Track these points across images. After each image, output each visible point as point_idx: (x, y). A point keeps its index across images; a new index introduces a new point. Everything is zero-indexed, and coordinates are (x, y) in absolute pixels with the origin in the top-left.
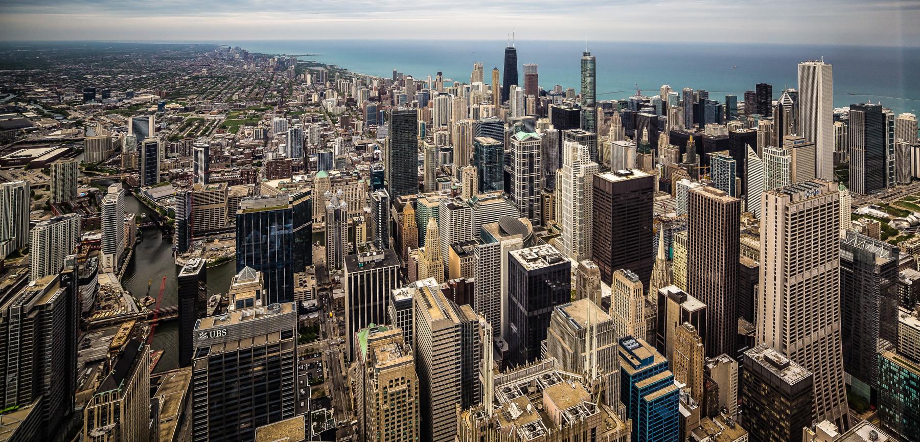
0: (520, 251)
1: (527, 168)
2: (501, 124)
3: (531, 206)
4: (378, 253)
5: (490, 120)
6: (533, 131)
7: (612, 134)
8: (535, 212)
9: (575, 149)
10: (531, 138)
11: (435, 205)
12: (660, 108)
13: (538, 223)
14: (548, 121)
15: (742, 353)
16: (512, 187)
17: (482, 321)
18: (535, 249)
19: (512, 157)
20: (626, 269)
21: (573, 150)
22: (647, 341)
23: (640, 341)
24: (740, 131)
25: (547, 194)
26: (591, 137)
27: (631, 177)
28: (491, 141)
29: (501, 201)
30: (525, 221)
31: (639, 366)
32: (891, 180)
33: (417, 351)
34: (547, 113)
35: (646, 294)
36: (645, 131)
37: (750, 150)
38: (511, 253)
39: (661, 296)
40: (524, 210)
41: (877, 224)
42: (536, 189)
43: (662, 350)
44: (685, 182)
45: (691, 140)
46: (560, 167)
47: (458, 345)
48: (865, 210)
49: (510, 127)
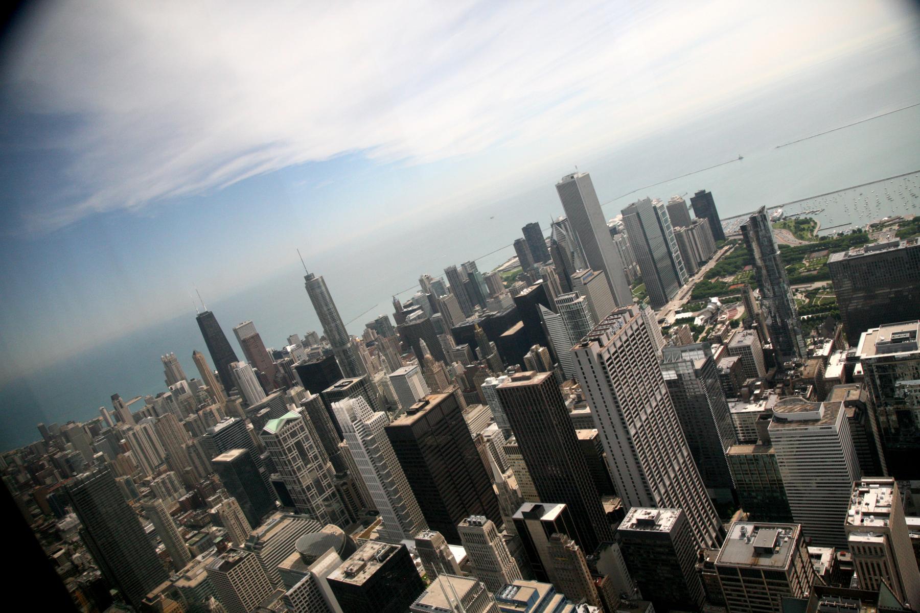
1: (300, 462)
6: (287, 411)
10: (289, 421)
12: (427, 305)
13: (347, 522)
14: (299, 389)
16: (293, 496)
18: (357, 556)
19: (275, 459)
24: (525, 292)
26: (361, 383)
27: (428, 407)
28: (235, 453)
29: (287, 522)
32: (683, 275)
36: (423, 343)
37: (543, 309)
38: (332, 576)
41: (686, 328)
42: (324, 483)
44: (492, 381)
45: (479, 330)
48: (671, 319)
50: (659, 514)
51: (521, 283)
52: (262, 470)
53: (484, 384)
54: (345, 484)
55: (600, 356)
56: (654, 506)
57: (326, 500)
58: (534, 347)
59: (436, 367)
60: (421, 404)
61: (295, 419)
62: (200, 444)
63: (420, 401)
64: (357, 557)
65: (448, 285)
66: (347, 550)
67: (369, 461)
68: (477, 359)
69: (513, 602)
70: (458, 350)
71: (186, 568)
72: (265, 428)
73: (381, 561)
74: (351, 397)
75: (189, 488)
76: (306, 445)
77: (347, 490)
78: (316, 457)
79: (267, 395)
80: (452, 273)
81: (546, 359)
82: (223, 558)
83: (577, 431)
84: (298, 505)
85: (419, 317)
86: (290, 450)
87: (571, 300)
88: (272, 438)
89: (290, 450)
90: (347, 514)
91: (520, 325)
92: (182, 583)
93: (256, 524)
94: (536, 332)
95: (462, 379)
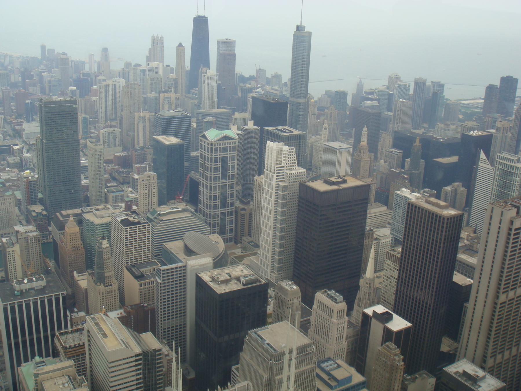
0: (209, 273)
1: (219, 174)
2: (188, 119)
3: (223, 220)
4: (37, 280)
5: (172, 113)
6: (228, 128)
7: (325, 132)
8: (228, 227)
9: (280, 152)
10: (226, 138)
11: (105, 220)
13: (230, 240)
14: (247, 115)
15: (441, 369)
16: (200, 197)
17: (166, 350)
19: (201, 161)
20: (330, 289)
21: (277, 153)
22: (346, 362)
23: (339, 362)
24: (475, 133)
25: (242, 206)
26: (299, 137)
27: (344, 186)
28: (173, 140)
29: (186, 214)
30: (216, 239)
31: (336, 387)
33: (92, 383)
34: (245, 103)
35: (348, 315)
37: (482, 155)
39: (365, 316)
40: (214, 226)
42: (229, 200)
43: (361, 370)
45: (417, 143)
46: (260, 172)
47: (140, 374)
49: (198, 122)
50: (484, 377)
51: (474, 123)
52: (186, 164)
53: (398, 192)
54: (244, 209)
55: (512, 222)
56: (483, 368)
57: (223, 214)
58: (456, 184)
59: (366, 157)
60: (340, 180)
61: (232, 139)
62: (150, 119)
63: (339, 177)
64: (227, 271)
65: (411, 91)
66: (220, 262)
67: (273, 202)
68: (403, 167)
69: (328, 373)
70: (391, 152)
71: (97, 207)
72: (207, 133)
73: (244, 285)
74: (285, 145)
75: (125, 149)
76: (230, 163)
77: (244, 215)
78: (233, 177)
79: (219, 108)
80: (420, 84)
81: (461, 199)
82: (127, 215)
83: (455, 272)
84: (200, 206)
85: (373, 107)
86: (216, 160)
87: (512, 161)
88: (208, 144)
89: (216, 160)
90: (233, 234)
91: (455, 159)
92: (87, 216)
93: (161, 203)
94: (466, 173)
95: (382, 178)
